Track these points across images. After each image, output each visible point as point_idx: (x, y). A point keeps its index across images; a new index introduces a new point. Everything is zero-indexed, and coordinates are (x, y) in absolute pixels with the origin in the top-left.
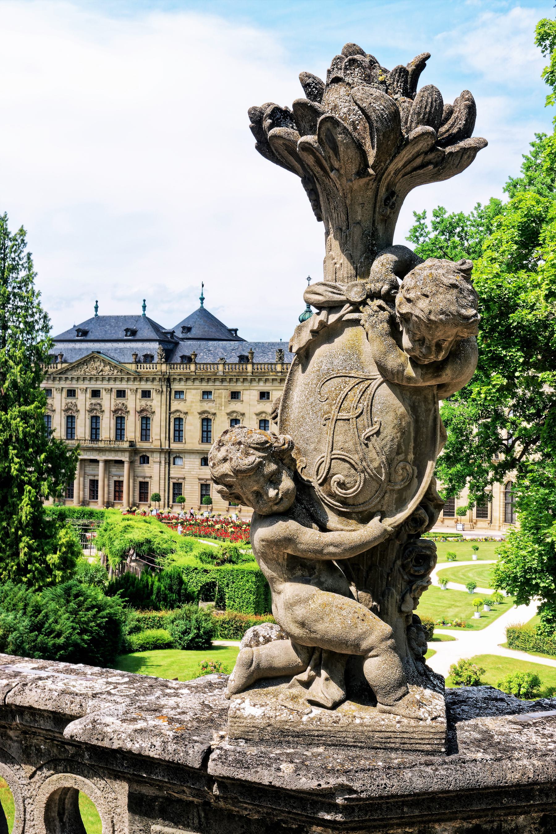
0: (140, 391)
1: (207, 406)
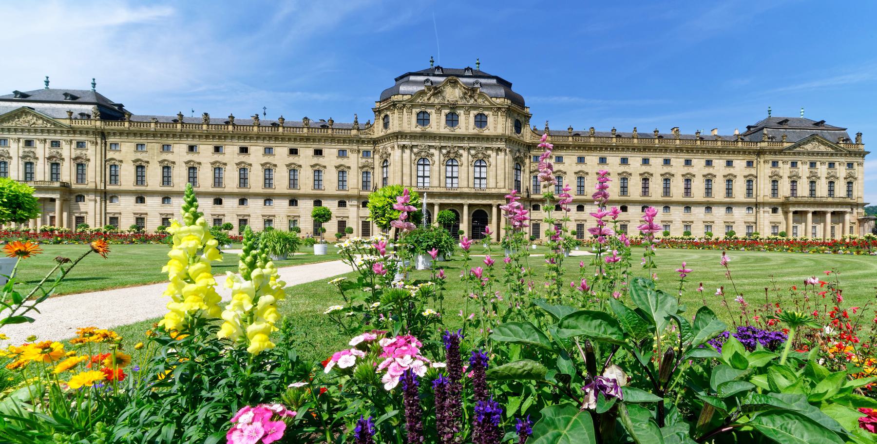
0: (74, 143)
1: (140, 156)
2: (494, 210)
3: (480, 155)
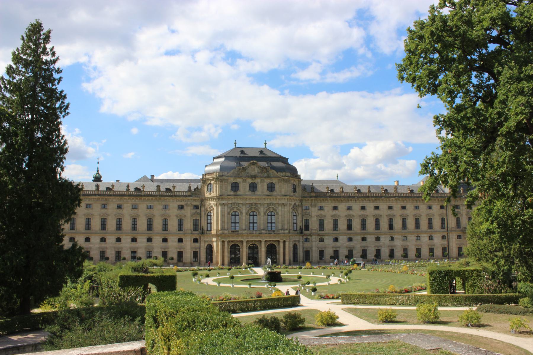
2: (281, 245)
3: (271, 210)
